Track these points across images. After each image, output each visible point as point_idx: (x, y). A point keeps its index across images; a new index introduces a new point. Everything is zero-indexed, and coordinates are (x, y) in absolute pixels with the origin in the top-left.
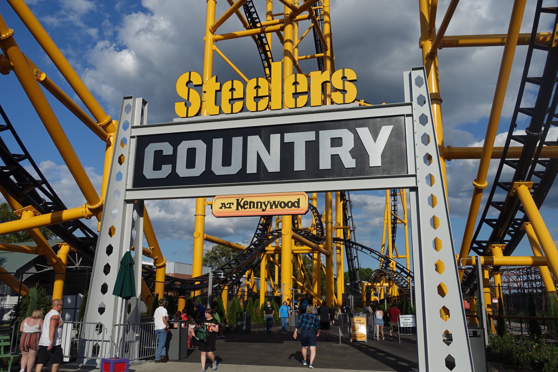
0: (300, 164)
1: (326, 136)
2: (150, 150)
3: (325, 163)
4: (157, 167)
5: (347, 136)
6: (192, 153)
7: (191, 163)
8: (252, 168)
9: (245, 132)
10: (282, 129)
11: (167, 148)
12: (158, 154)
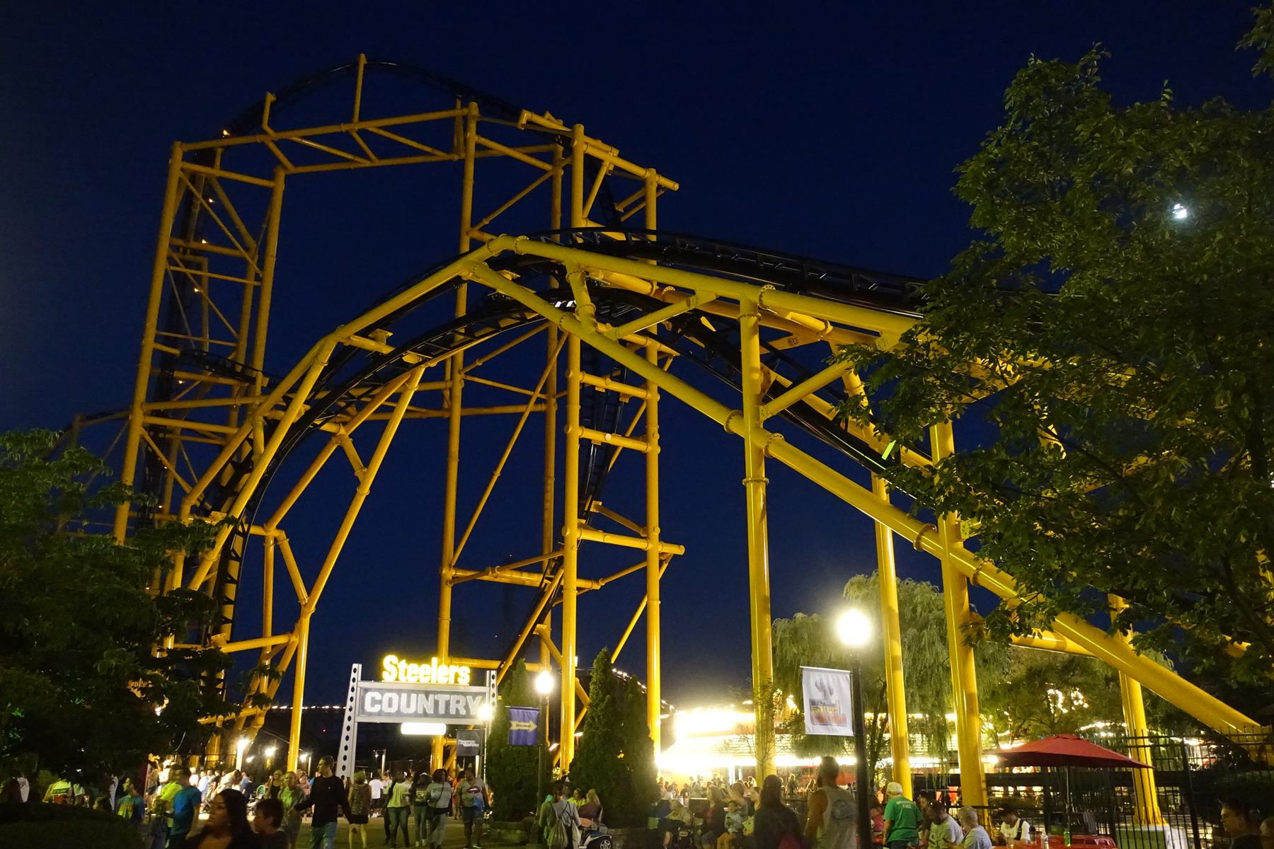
0: (442, 710)
1: (453, 698)
2: (369, 696)
3: (453, 712)
4: (373, 705)
5: (461, 698)
6: (390, 700)
7: (390, 705)
8: (420, 711)
9: (417, 692)
10: (435, 693)
11: (377, 696)
12: (373, 699)
